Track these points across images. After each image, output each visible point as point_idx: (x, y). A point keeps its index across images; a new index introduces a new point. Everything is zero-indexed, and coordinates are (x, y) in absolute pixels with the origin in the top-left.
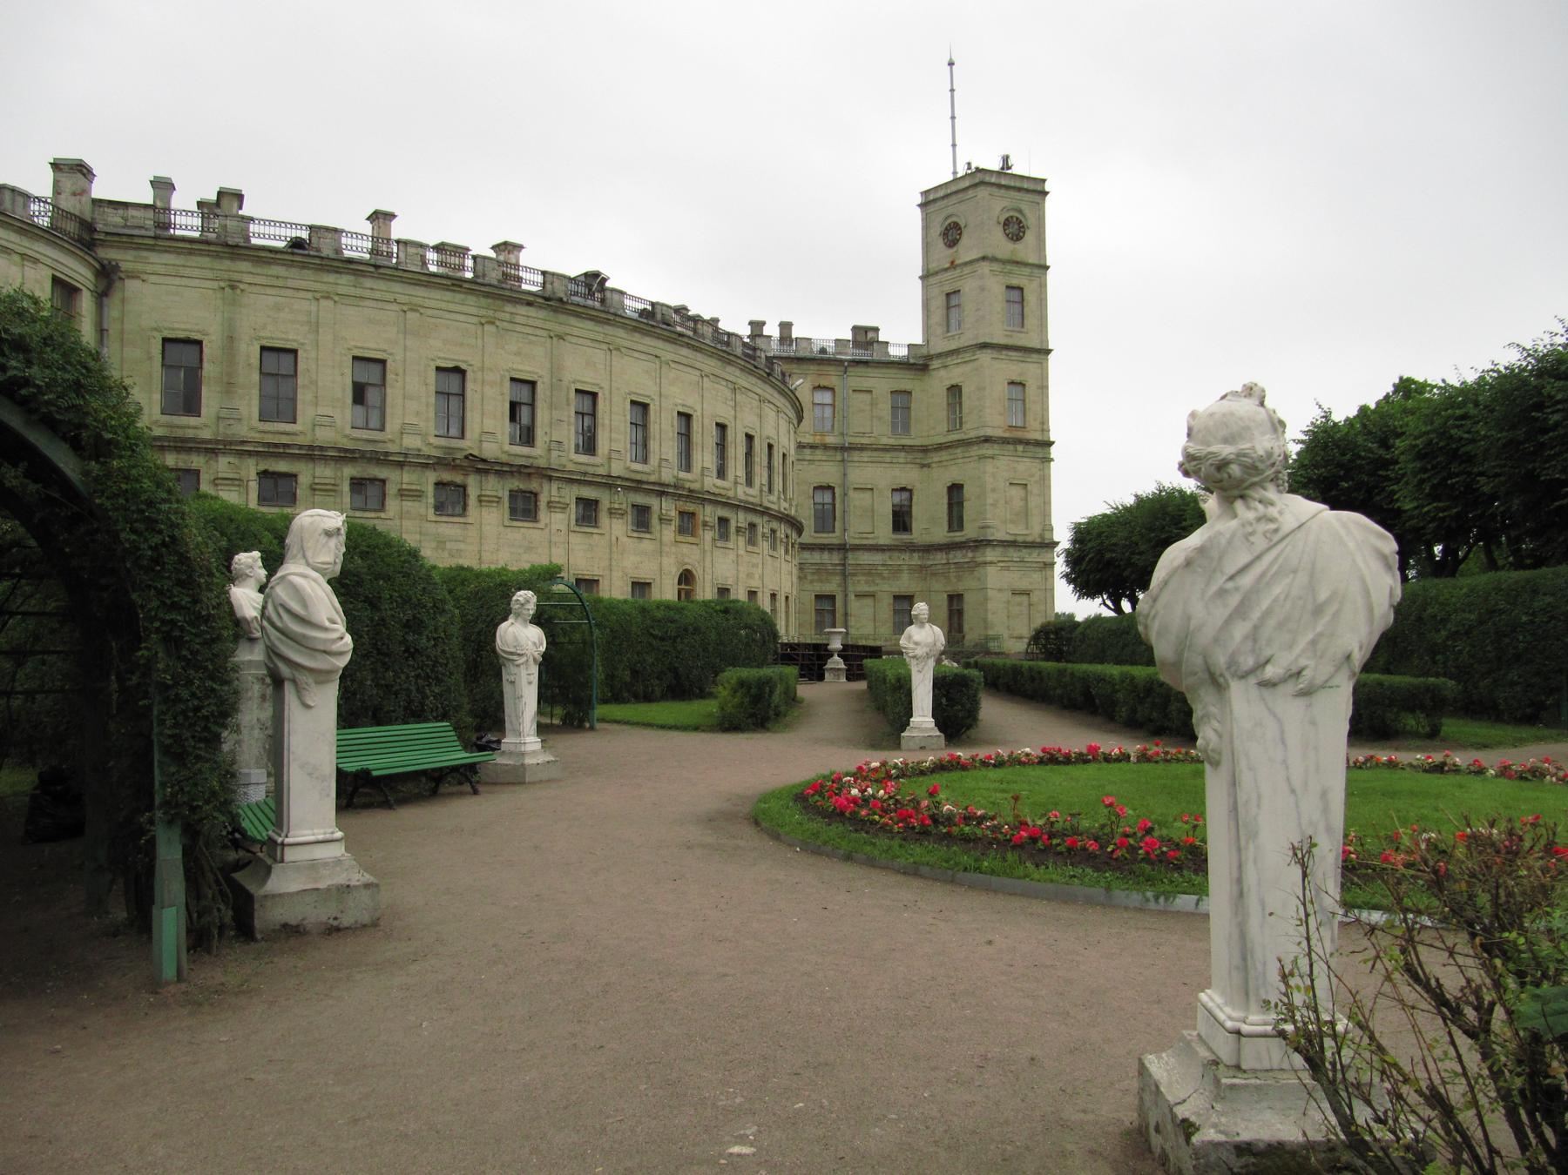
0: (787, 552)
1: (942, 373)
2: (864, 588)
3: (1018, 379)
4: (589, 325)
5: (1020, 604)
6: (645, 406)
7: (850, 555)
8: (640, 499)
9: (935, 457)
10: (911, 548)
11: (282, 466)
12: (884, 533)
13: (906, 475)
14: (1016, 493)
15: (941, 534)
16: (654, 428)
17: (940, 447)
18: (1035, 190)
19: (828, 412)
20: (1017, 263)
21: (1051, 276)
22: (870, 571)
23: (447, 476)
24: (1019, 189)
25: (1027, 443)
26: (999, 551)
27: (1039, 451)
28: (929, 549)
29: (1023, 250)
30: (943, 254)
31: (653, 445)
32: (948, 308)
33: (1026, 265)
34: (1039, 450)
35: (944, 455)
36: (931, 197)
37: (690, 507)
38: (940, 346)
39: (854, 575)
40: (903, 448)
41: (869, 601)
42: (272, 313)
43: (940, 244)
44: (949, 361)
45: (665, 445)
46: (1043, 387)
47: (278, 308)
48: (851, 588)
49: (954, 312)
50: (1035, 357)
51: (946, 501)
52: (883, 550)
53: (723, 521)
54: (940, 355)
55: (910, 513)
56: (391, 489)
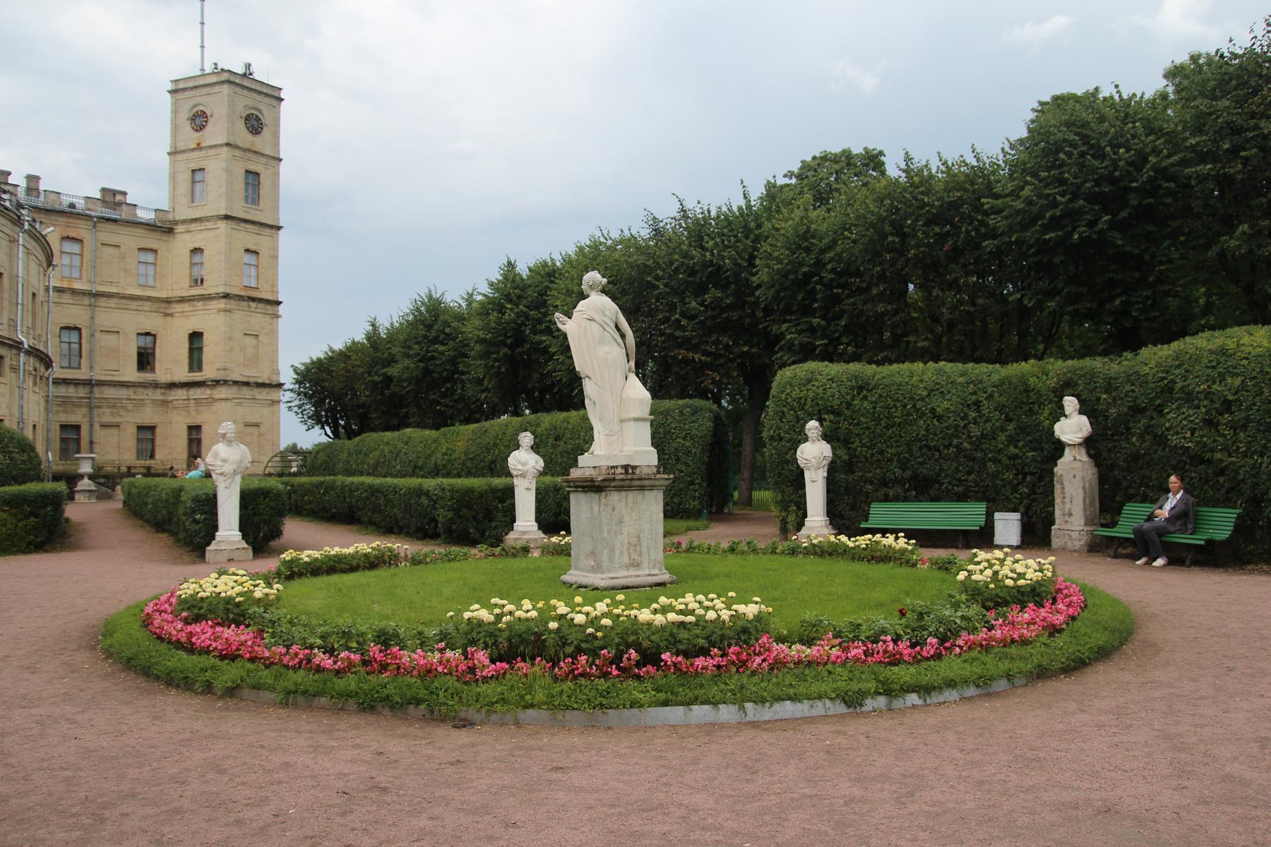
0: (35, 384)
1: (187, 237)
2: (108, 419)
3: (252, 248)
5: (251, 434)
7: (96, 389)
9: (178, 308)
10: (156, 385)
12: (130, 372)
13: (151, 322)
14: (248, 340)
15: (183, 374)
17: (182, 300)
19: (77, 261)
21: (283, 167)
22: (115, 405)
24: (260, 93)
25: (261, 300)
26: (235, 389)
27: (270, 309)
28: (172, 386)
30: (190, 137)
32: (193, 182)
33: (263, 155)
34: (269, 307)
35: (186, 307)
36: (181, 86)
38: (184, 213)
39: (100, 407)
40: (148, 299)
41: (114, 431)
43: (187, 128)
44: (193, 227)
46: (275, 257)
48: (96, 419)
49: (198, 187)
50: (268, 231)
51: (187, 345)
52: (128, 386)
54: (184, 222)
55: (153, 354)
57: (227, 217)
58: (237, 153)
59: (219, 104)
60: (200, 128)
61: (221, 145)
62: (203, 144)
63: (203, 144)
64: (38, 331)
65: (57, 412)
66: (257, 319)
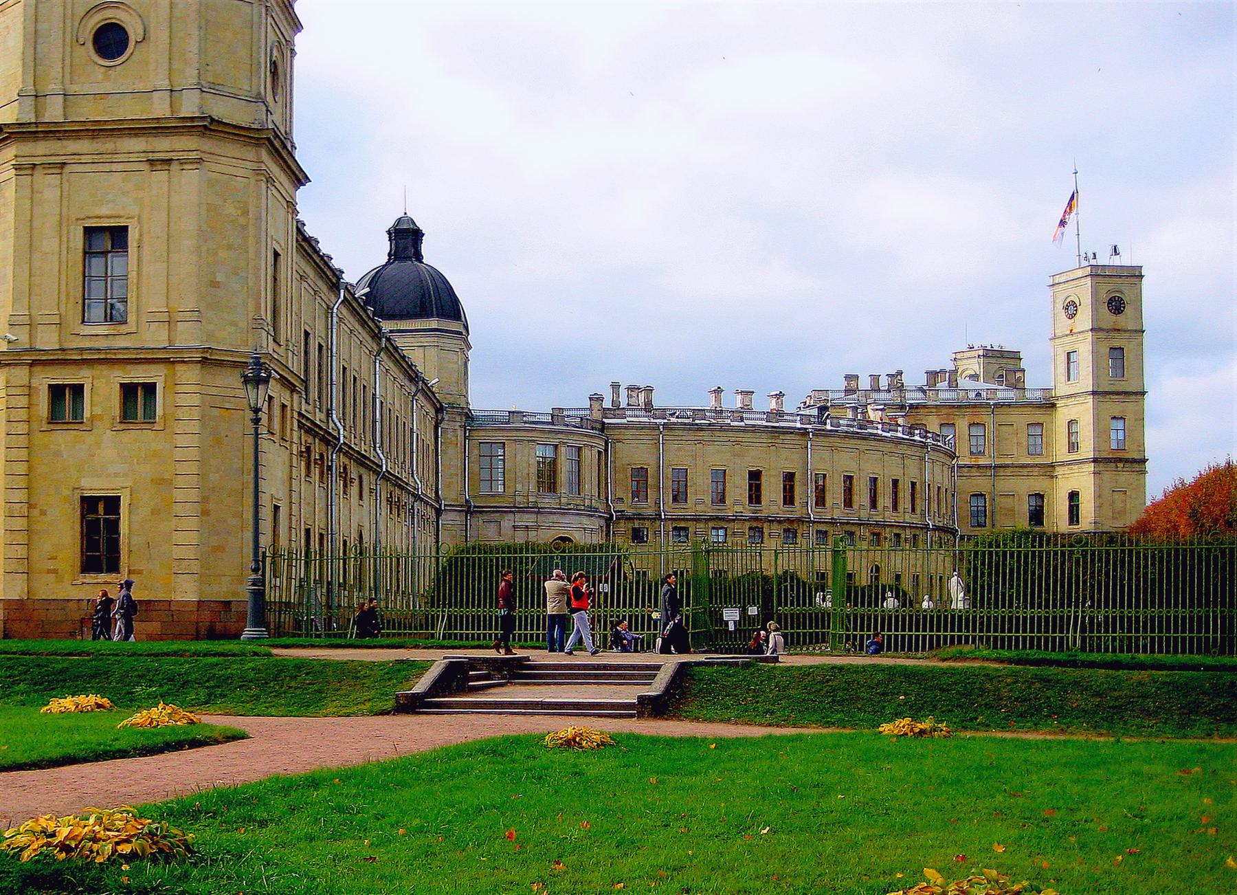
1: (1065, 410)
4: (821, 439)
6: (850, 478)
8: (847, 528)
11: (682, 525)
14: (1116, 496)
16: (855, 489)
17: (1063, 464)
18: (1135, 275)
19: (981, 441)
23: (755, 525)
25: (1127, 461)
27: (1136, 467)
30: (1064, 323)
31: (855, 498)
37: (877, 530)
42: (678, 454)
45: (861, 496)
47: (679, 450)
53: (898, 535)
54: (1062, 397)
56: (729, 532)
58: (1102, 335)
59: (1084, 293)
60: (1072, 316)
64: (943, 510)
66: (1125, 477)
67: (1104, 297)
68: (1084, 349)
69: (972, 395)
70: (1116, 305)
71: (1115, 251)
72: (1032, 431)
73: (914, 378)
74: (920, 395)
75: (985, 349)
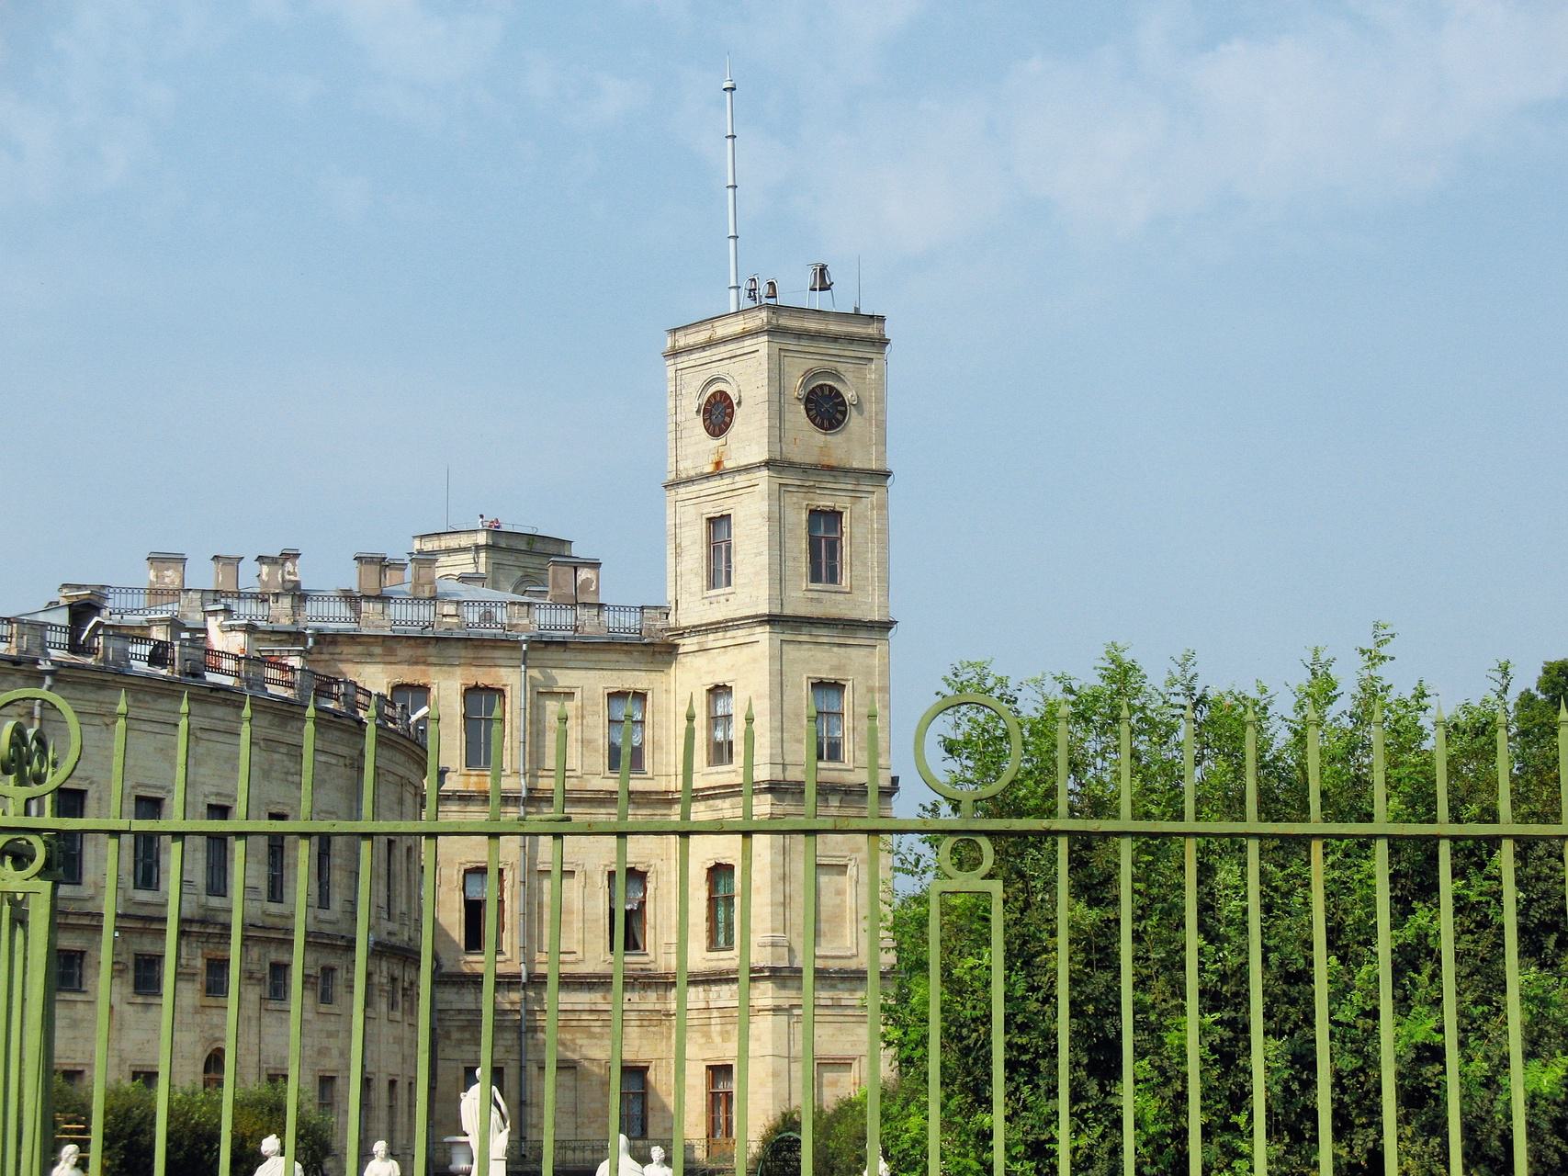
0: (393, 1006)
1: (700, 660)
3: (827, 675)
12: (593, 954)
18: (865, 335)
20: (831, 468)
29: (846, 447)
30: (698, 448)
33: (847, 471)
44: (711, 640)
54: (697, 630)
57: (772, 620)
59: (749, 375)
61: (758, 467)
62: (728, 464)
63: (728, 464)
65: (460, 1042)
67: (795, 386)
68: (751, 510)
69: (472, 616)
70: (826, 408)
71: (823, 281)
72: (622, 710)
73: (326, 571)
74: (343, 610)
75: (495, 531)
